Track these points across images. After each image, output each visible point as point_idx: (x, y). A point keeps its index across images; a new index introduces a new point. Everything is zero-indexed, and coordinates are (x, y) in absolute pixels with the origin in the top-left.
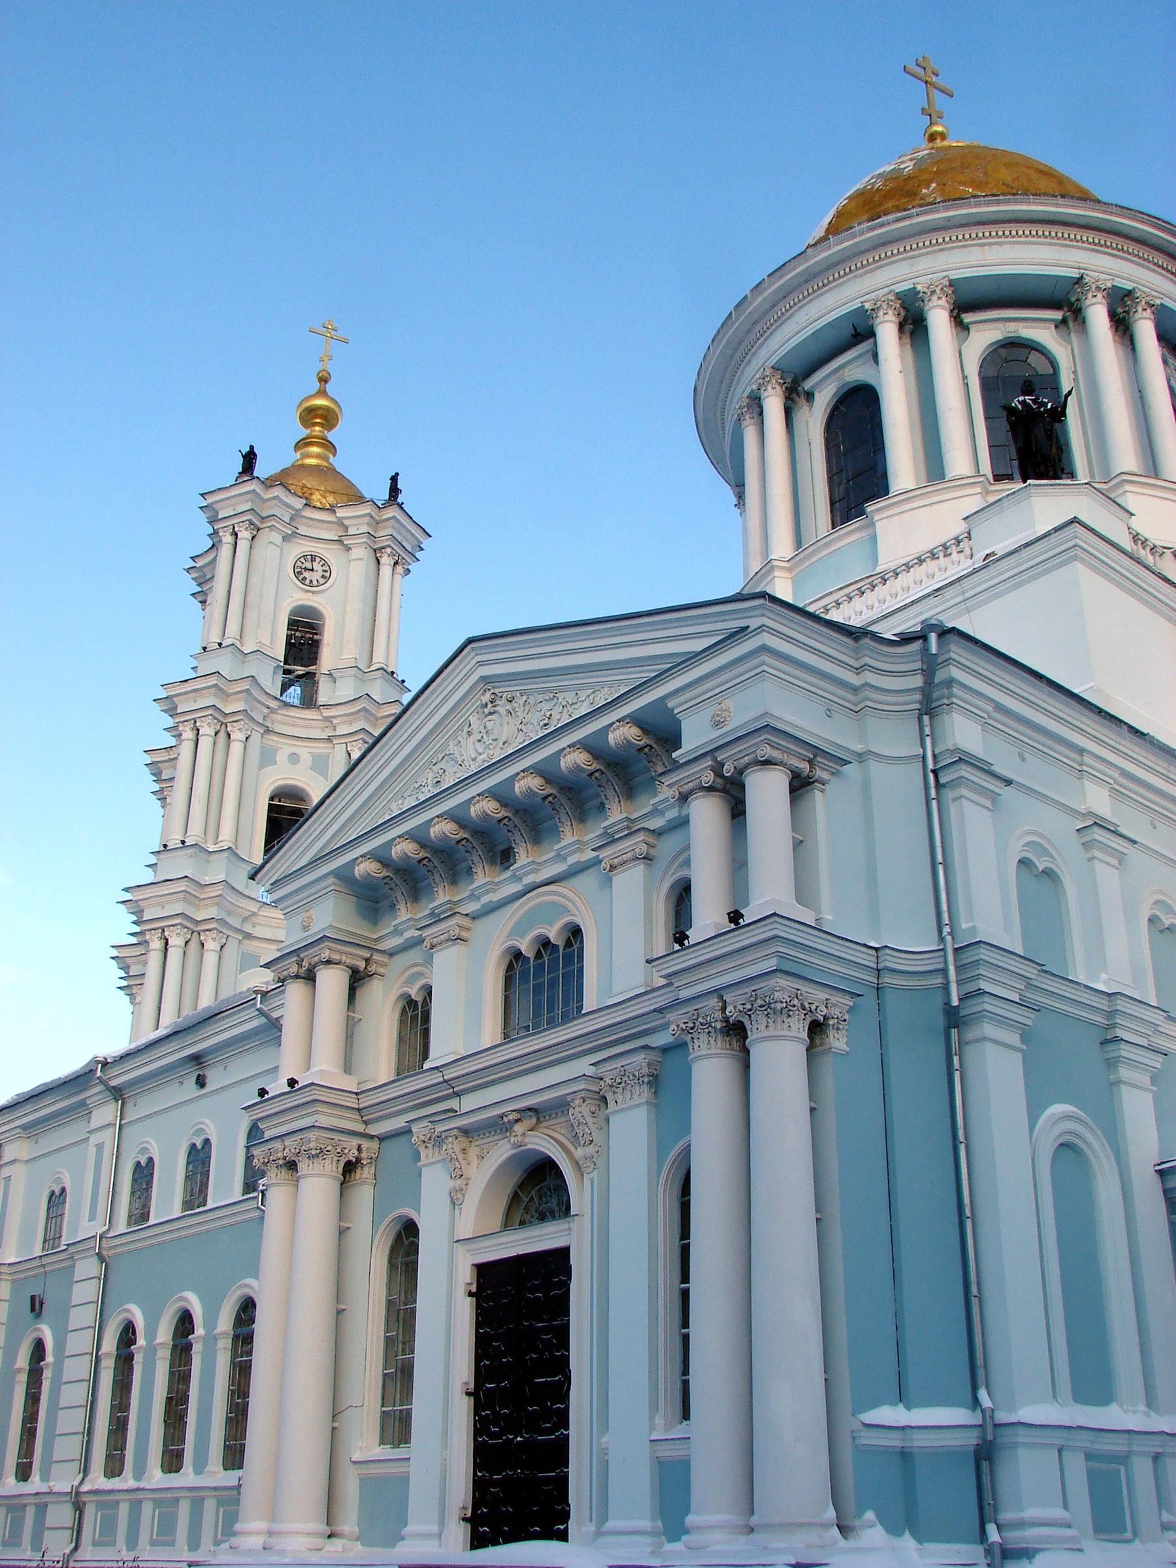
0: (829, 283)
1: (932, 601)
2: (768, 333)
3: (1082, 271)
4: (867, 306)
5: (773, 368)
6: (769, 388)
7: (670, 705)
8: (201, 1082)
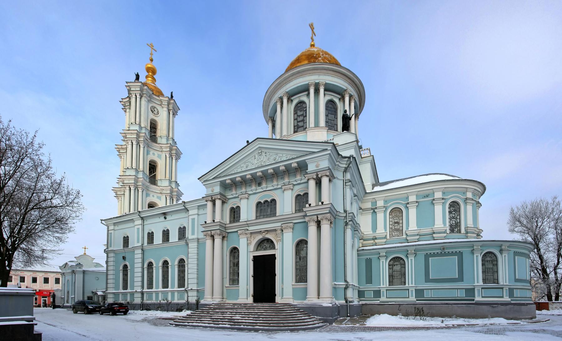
5: (287, 92)
7: (306, 161)
8: (165, 218)
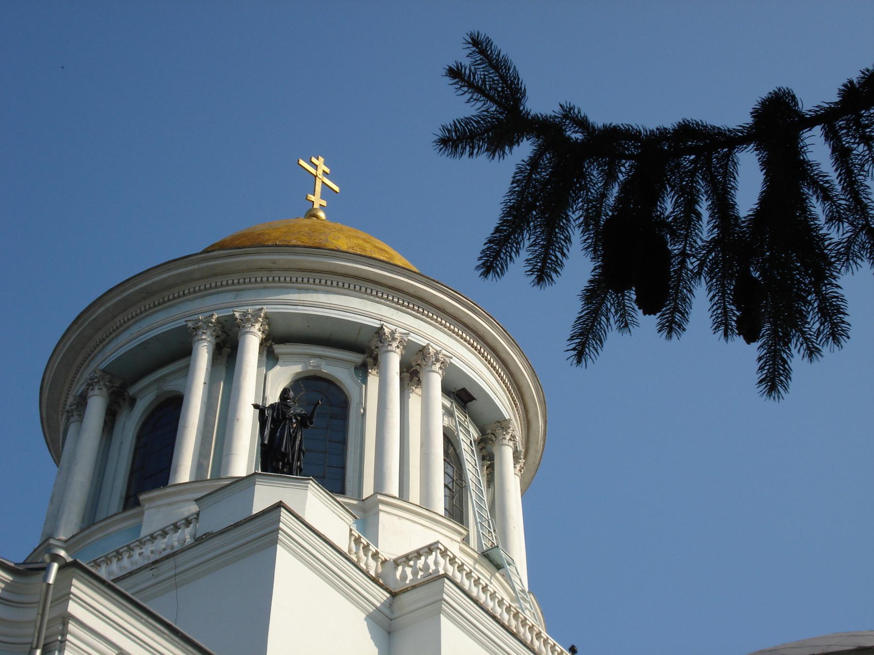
0: (164, 302)
1: (147, 574)
2: (107, 340)
3: (382, 322)
4: (190, 324)
5: (103, 371)
6: (96, 388)
